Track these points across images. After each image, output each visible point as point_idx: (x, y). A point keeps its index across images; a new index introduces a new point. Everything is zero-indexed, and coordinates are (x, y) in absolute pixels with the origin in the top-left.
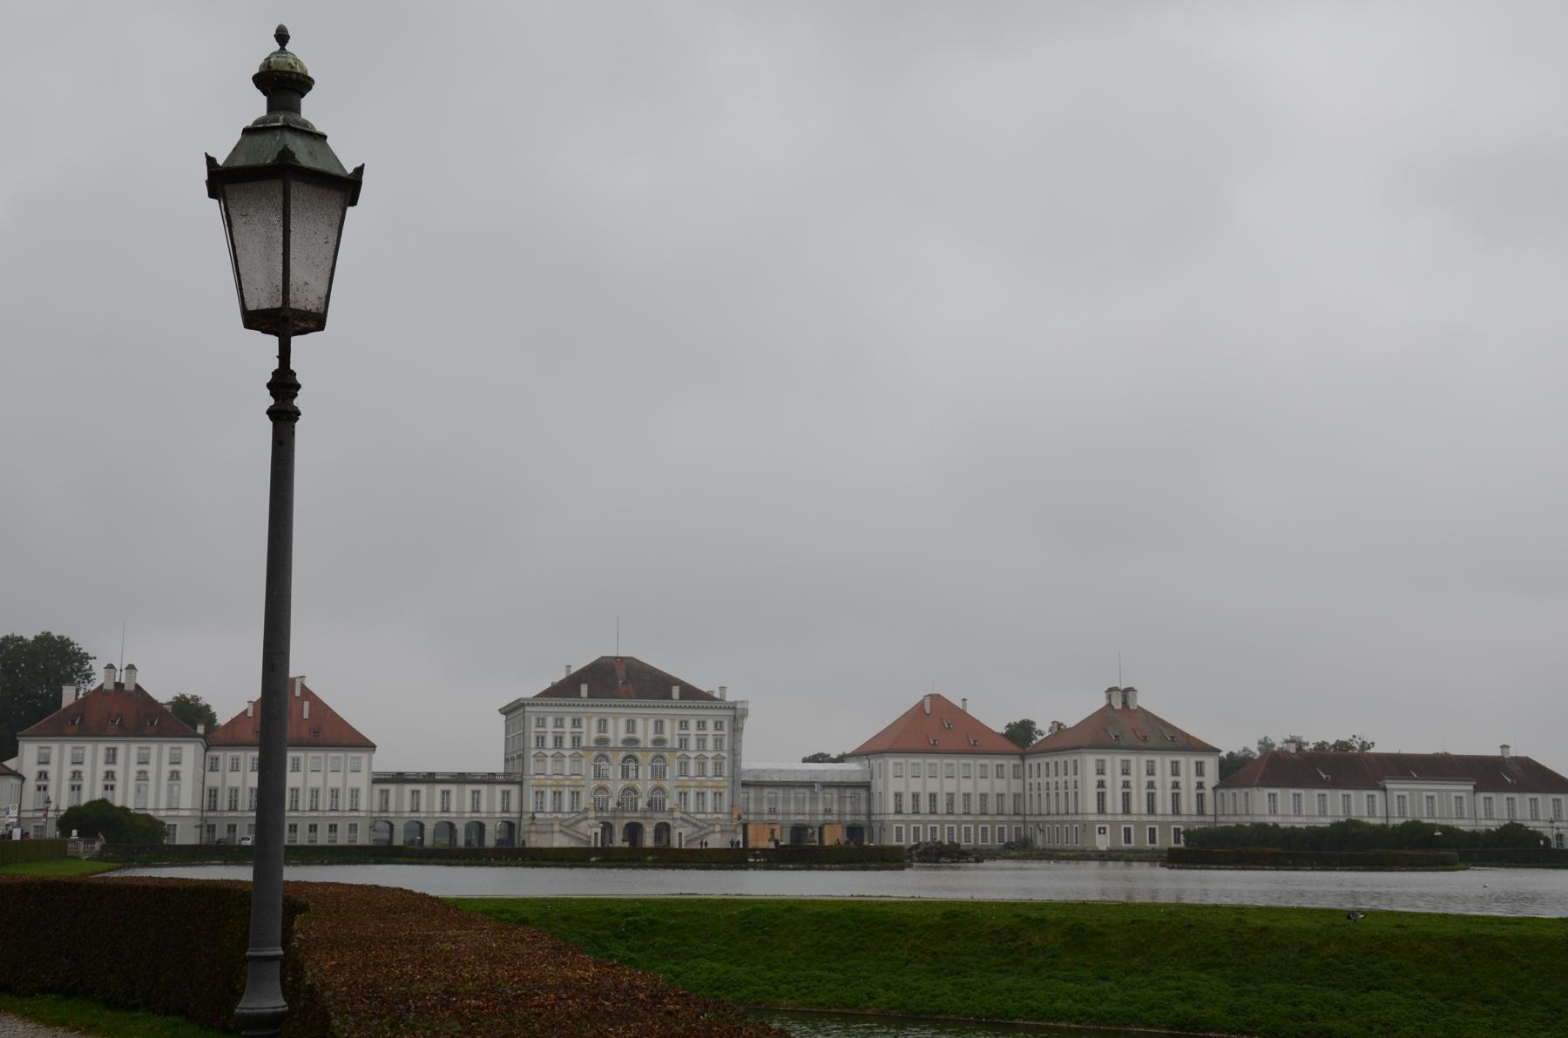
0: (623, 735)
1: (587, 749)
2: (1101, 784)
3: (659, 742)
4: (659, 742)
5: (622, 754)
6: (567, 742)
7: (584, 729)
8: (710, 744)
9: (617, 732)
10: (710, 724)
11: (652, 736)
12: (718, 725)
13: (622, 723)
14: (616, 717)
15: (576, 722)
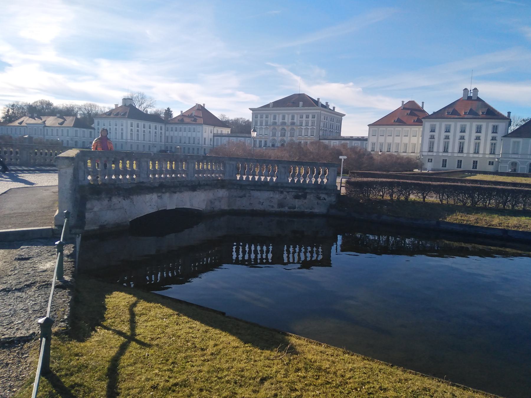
0: (281, 121)
1: (270, 126)
2: (432, 137)
3: (293, 124)
4: (293, 124)
5: (280, 127)
6: (264, 124)
7: (269, 119)
8: (310, 124)
9: (279, 120)
10: (311, 116)
11: (290, 121)
12: (313, 117)
13: (281, 116)
14: (279, 114)
15: (267, 117)
